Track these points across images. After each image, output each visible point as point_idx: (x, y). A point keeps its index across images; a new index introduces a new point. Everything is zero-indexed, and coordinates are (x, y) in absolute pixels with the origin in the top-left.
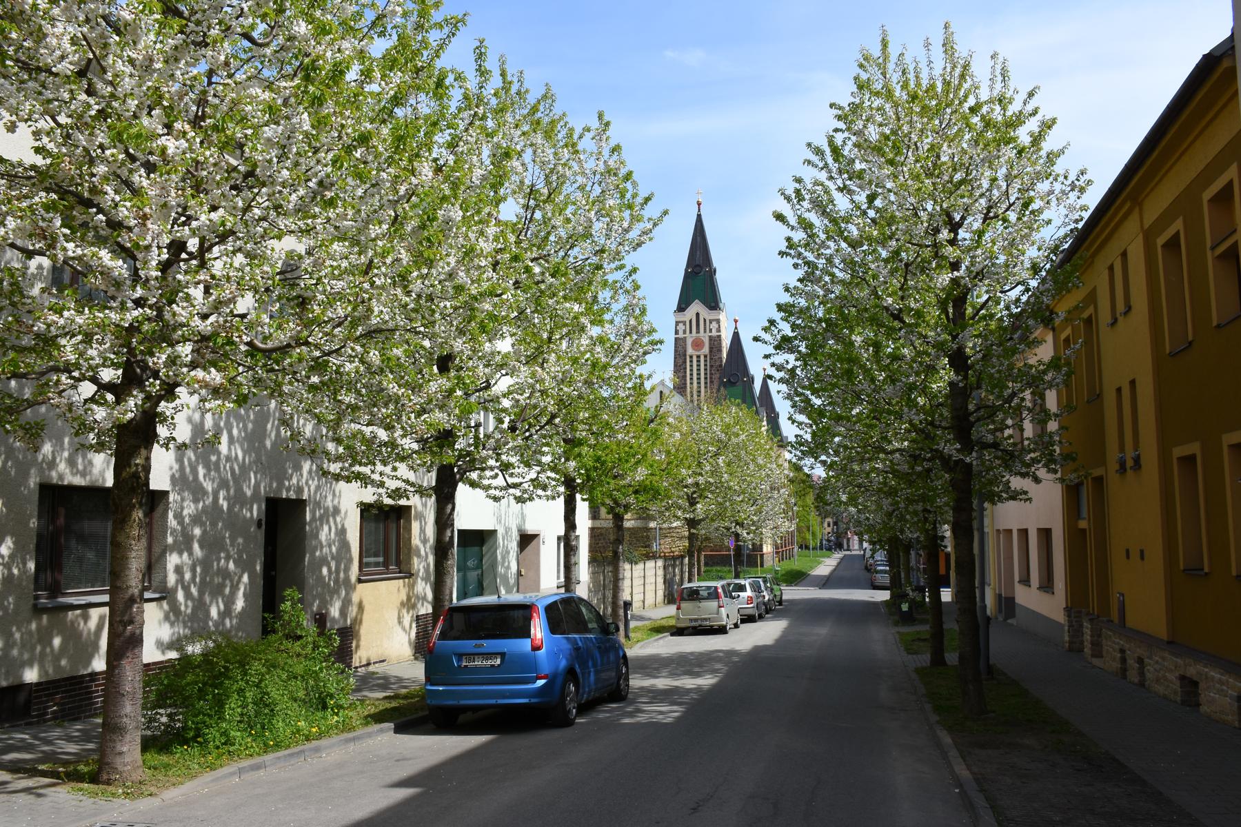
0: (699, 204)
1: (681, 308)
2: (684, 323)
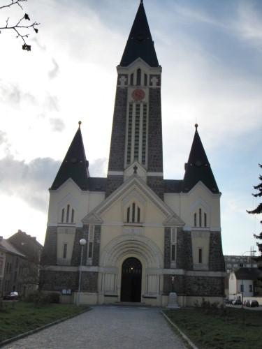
2: (126, 76)
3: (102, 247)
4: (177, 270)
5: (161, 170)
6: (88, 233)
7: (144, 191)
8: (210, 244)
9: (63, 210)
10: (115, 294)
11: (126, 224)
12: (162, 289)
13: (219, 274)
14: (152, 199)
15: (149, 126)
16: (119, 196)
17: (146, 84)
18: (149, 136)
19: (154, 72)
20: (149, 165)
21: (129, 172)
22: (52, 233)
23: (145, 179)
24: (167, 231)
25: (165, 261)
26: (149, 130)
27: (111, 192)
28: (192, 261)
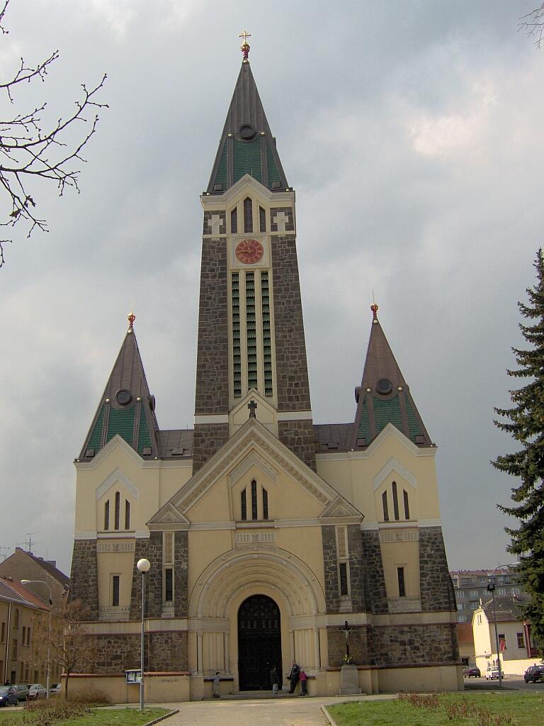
0: (246, 50)
1: (218, 185)
2: (222, 214)
3: (194, 576)
4: (354, 615)
5: (308, 408)
6: (160, 549)
7: (272, 453)
8: (421, 556)
9: (107, 504)
10: (230, 677)
11: (239, 525)
12: (325, 657)
13: (444, 617)
14: (291, 470)
15: (277, 317)
16: (221, 467)
17: (263, 229)
18: (276, 337)
19: (281, 201)
20: (280, 399)
21: (241, 414)
22: (85, 552)
23: (275, 429)
24: (328, 534)
25: (327, 598)
26: (276, 323)
27: (205, 459)
28: (385, 595)
